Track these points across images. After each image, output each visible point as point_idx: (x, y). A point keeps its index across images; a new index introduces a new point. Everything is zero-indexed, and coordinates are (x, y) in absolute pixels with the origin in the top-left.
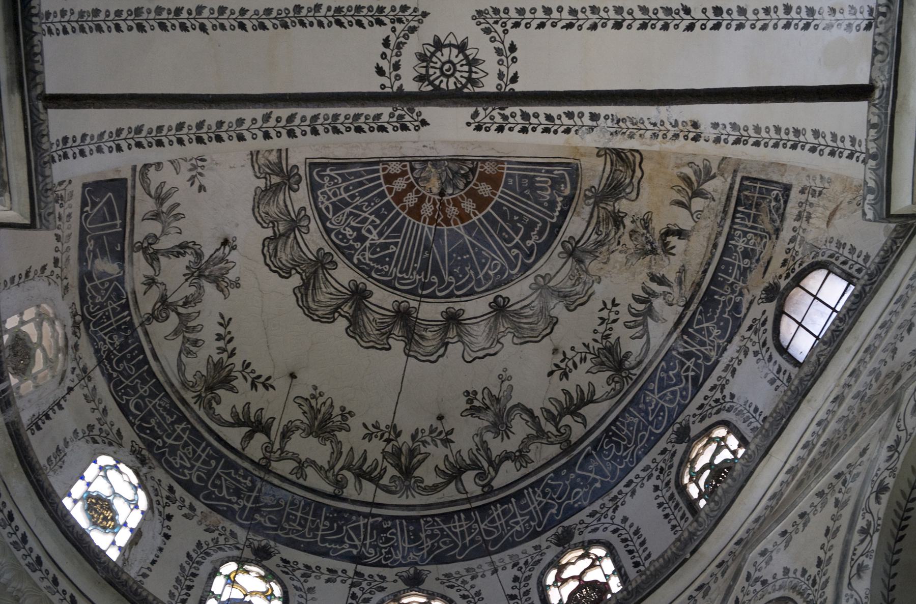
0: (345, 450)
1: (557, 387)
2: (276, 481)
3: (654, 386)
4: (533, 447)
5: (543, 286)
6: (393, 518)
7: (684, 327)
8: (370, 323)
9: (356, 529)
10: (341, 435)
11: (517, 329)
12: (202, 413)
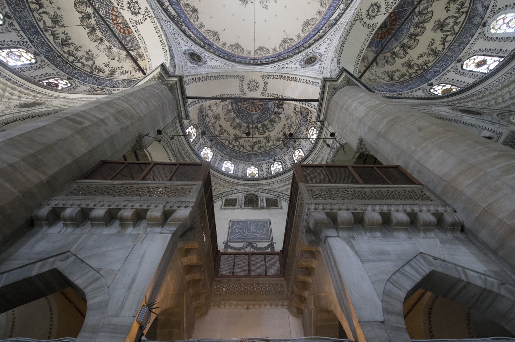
0: (55, 29)
1: (102, 66)
2: (31, 14)
5: (119, 54)
7: (124, 81)
8: (86, 22)
9: (38, 38)
11: (109, 53)
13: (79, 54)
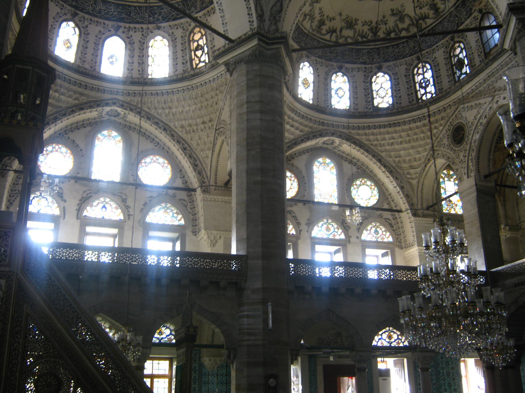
0: (357, 30)
3: (446, 20)
4: (411, 27)
6: (372, 49)
9: (363, 54)
10: (356, 27)
12: (319, 35)
13: (391, 23)
